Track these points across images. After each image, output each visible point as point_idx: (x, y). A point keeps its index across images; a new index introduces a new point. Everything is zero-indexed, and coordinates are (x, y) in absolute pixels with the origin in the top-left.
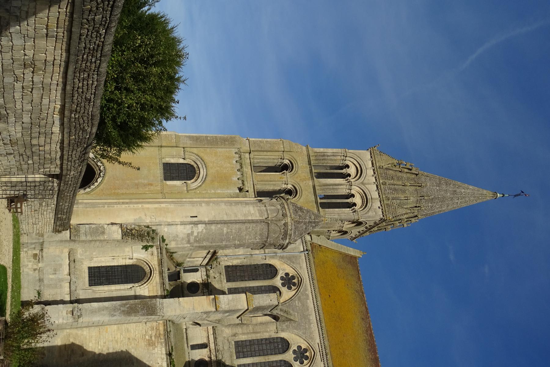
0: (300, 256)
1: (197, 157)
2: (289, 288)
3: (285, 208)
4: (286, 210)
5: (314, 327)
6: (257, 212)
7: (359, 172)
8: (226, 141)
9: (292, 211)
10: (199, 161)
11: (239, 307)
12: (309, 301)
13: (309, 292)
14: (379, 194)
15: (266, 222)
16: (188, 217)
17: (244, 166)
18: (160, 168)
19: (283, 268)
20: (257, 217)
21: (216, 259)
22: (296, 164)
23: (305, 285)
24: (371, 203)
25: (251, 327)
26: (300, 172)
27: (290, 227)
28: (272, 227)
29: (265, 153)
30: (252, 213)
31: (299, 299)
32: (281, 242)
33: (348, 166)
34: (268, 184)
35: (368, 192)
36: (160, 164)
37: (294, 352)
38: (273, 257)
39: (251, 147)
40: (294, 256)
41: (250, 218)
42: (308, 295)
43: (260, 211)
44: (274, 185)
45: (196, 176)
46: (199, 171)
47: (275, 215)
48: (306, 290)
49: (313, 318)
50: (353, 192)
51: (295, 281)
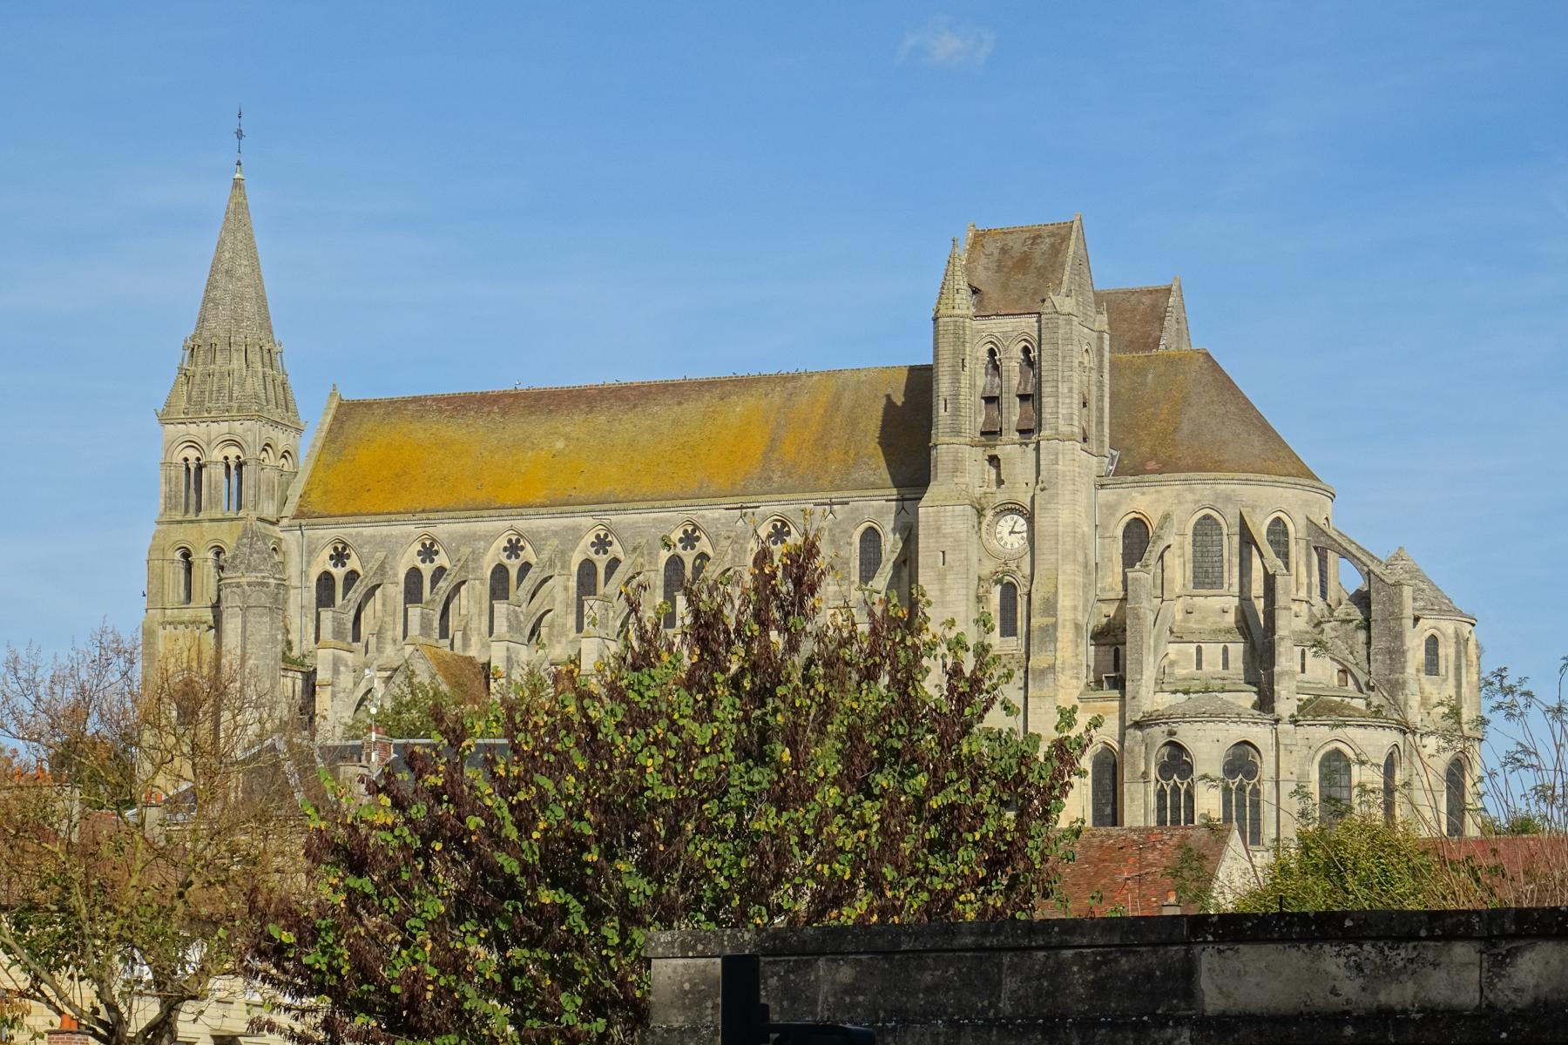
0: (309, 537)
2: (348, 557)
5: (396, 530)
9: (234, 575)
11: (331, 658)
12: (365, 533)
13: (354, 531)
15: (245, 610)
17: (182, 619)
19: (323, 562)
20: (239, 620)
21: (304, 656)
25: (387, 619)
26: (191, 539)
27: (253, 579)
28: (252, 602)
29: (166, 586)
31: (361, 546)
32: (272, 587)
33: (186, 460)
34: (208, 582)
37: (423, 561)
38: (307, 576)
40: (308, 546)
41: (240, 630)
42: (358, 533)
43: (234, 616)
44: (208, 575)
49: (385, 530)
50: (221, 459)
51: (340, 547)
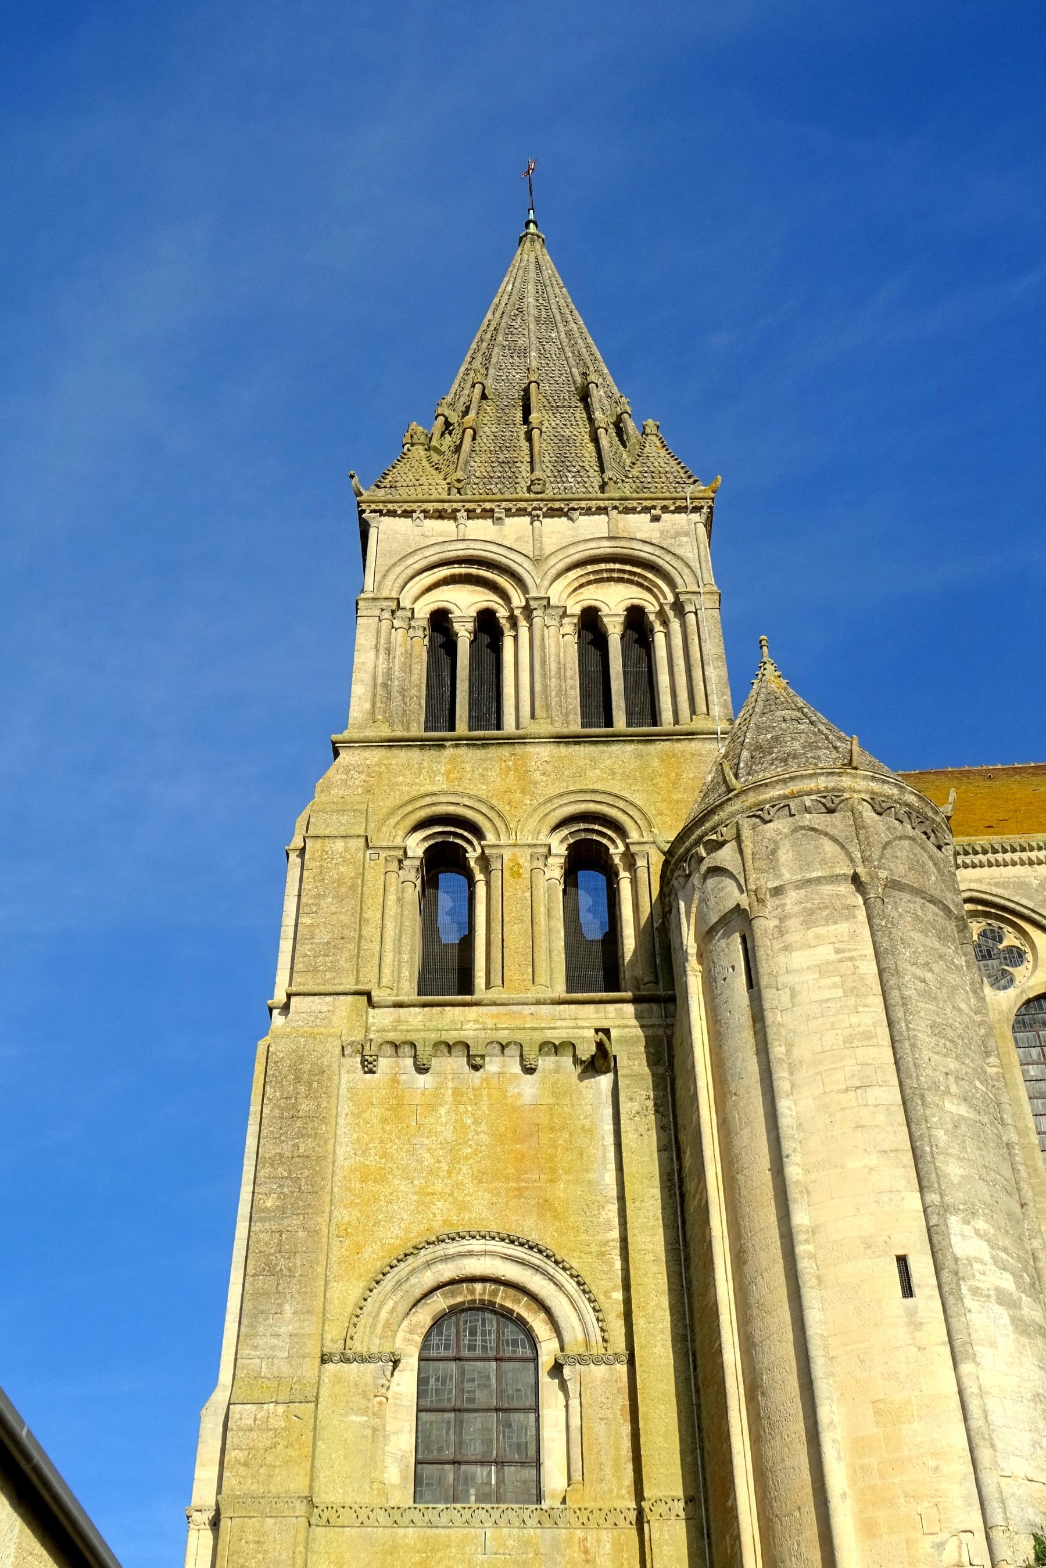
1: (388, 1283)
3: (785, 797)
4: (801, 794)
6: (821, 930)
7: (474, 571)
8: (294, 1106)
10: (413, 1272)
14: (588, 512)
16: (912, 1313)
18: (459, 1521)
22: (434, 799)
23: (997, 885)
24: (635, 545)
30: (833, 957)
35: (582, 547)
36: (431, 1525)
39: (340, 989)
45: (509, 1304)
46: (479, 1286)
47: (829, 848)
48: (1021, 885)
